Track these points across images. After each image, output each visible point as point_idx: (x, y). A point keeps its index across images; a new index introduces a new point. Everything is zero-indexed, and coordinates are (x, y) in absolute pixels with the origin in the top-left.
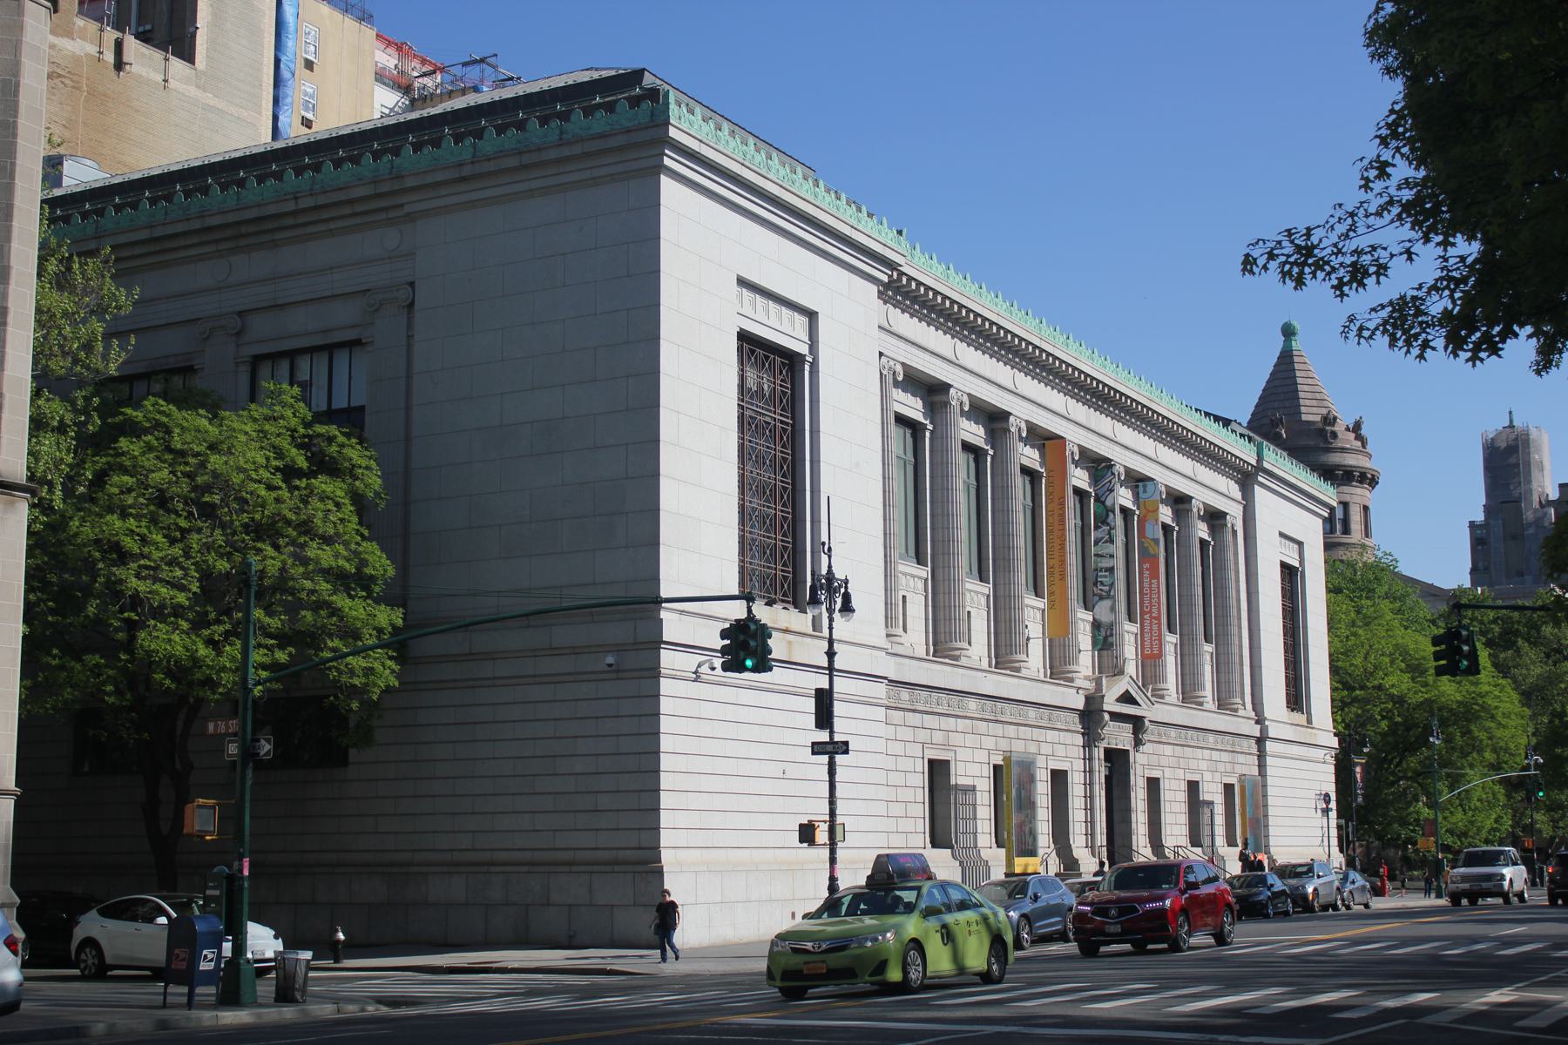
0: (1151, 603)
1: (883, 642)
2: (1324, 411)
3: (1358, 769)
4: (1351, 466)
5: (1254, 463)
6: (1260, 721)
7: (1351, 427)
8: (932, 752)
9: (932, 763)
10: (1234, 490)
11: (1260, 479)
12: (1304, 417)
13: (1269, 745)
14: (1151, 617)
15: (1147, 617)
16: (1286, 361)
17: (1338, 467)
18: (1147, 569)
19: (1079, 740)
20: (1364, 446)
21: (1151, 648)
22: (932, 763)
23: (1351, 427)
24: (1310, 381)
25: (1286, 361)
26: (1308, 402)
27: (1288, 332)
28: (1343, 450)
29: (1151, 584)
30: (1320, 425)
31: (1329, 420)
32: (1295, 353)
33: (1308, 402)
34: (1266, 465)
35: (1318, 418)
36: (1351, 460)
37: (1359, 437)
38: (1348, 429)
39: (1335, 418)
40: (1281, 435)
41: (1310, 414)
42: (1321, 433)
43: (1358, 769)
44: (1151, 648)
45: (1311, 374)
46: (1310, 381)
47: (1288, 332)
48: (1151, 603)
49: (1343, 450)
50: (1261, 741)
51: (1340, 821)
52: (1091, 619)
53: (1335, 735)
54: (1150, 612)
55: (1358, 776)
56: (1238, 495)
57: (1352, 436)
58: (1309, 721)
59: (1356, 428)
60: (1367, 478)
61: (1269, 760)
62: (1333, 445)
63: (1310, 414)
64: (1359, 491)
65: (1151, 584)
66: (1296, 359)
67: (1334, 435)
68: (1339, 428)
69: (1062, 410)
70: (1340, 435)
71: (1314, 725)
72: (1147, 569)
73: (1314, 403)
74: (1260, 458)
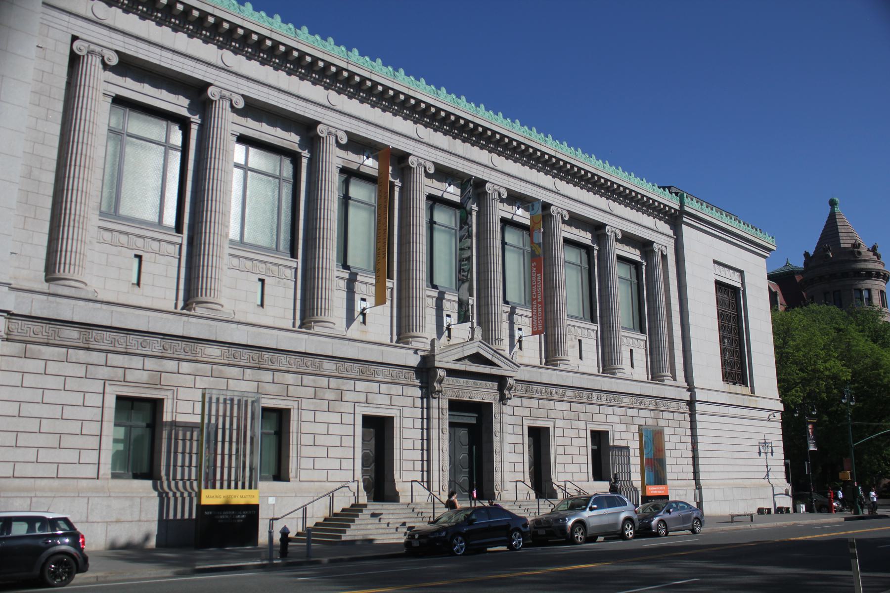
0: (537, 292)
1: (45, 287)
2: (853, 242)
3: (810, 426)
4: (870, 269)
5: (677, 207)
6: (691, 389)
7: (870, 249)
8: (528, 422)
9: (369, 421)
10: (666, 228)
11: (685, 219)
12: (842, 246)
13: (698, 407)
14: (537, 302)
15: (534, 303)
16: (832, 219)
17: (862, 270)
18: (535, 267)
19: (418, 392)
20: (878, 259)
21: (537, 326)
22: (369, 421)
23: (870, 249)
24: (846, 227)
25: (832, 218)
26: (844, 238)
27: (833, 203)
28: (865, 261)
29: (537, 277)
30: (852, 249)
31: (856, 246)
32: (836, 214)
33: (844, 238)
34: (686, 209)
35: (850, 246)
36: (870, 266)
37: (875, 254)
38: (869, 250)
39: (859, 244)
40: (829, 256)
41: (845, 243)
42: (852, 253)
43: (810, 426)
44: (537, 326)
45: (846, 224)
46: (846, 227)
47: (833, 203)
48: (537, 292)
49: (865, 261)
50: (691, 403)
51: (787, 461)
52: (456, 299)
53: (781, 402)
54: (537, 299)
55: (810, 431)
56: (671, 233)
57: (871, 254)
58: (753, 391)
59: (874, 249)
60: (881, 275)
61: (698, 417)
62: (860, 259)
63: (845, 243)
64: (877, 282)
65: (537, 277)
66: (837, 217)
67: (859, 253)
68: (863, 249)
69: (652, 226)
70: (863, 253)
71: (756, 394)
72: (535, 267)
73: (848, 238)
74: (682, 204)
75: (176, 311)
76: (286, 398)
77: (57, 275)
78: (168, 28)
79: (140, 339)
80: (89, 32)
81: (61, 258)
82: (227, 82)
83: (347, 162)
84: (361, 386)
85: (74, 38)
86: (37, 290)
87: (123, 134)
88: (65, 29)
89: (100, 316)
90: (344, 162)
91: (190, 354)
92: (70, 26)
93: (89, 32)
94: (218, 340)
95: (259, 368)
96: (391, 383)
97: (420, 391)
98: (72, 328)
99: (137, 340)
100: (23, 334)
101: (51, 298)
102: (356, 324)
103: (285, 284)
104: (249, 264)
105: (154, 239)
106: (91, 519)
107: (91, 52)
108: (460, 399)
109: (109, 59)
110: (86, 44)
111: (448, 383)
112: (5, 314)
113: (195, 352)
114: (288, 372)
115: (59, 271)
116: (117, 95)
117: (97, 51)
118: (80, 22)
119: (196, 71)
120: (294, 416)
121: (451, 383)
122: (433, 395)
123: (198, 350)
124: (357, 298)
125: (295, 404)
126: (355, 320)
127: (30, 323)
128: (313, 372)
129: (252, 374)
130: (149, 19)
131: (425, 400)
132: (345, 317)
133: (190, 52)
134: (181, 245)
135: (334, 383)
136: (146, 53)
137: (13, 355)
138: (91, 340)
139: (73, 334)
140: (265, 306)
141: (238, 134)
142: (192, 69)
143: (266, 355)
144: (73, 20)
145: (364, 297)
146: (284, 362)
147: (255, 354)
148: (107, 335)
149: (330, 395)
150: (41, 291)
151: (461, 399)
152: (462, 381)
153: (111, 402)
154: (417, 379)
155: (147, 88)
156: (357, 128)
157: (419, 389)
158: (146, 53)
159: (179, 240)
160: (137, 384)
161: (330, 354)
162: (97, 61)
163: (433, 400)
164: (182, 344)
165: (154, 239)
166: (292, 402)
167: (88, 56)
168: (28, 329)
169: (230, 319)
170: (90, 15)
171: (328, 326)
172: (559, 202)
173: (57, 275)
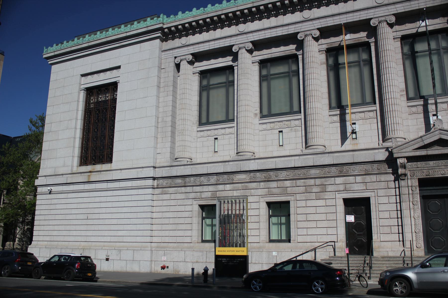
19: (392, 177)
75: (380, 147)
76: (367, 191)
77: (387, 137)
78: (342, 3)
79: (206, 178)
80: (180, 52)
81: (388, 128)
82: (242, 39)
83: (330, 44)
84: (339, 180)
85: (175, 57)
86: (165, 166)
87: (440, 49)
88: (172, 56)
89: (270, 164)
90: (328, 45)
91: (230, 180)
92: (173, 54)
93: (180, 52)
94: (242, 170)
95: (268, 181)
96: (365, 175)
97: (394, 176)
98: (179, 179)
99: (337, 169)
100: (335, 173)
101: (171, 168)
102: (348, 142)
103: (295, 130)
104: (272, 125)
105: (222, 128)
106: (186, 260)
107: (306, 36)
108: (430, 177)
109: (315, 35)
110: (377, 19)
111: (416, 167)
112: (152, 178)
113: (232, 179)
114: (286, 180)
115: (388, 135)
116: (260, 60)
117: (383, 20)
118: (177, 50)
119: (335, 21)
120: (372, 201)
121: (419, 166)
122: (401, 177)
123: (234, 177)
124: (348, 124)
125: (373, 194)
126: (347, 138)
127: (164, 180)
128: (304, 177)
129: (264, 185)
130: (232, 26)
131: (397, 182)
132: (340, 138)
133: (279, 24)
134: (376, 110)
135: (318, 181)
136: (203, 47)
137: (159, 193)
138: (186, 182)
139: (179, 181)
140: (357, 138)
141: (401, 36)
142: (270, 34)
143: (271, 173)
144: (174, 51)
145: (216, 137)
146: (282, 175)
147: (338, 168)
148: (192, 179)
149: (315, 189)
150: (167, 166)
151: (432, 176)
152: (431, 163)
153: (341, 203)
154: (389, 168)
155: (213, 61)
156: (326, 23)
157: (391, 175)
158: (203, 47)
159: (374, 108)
160: (206, 199)
161: (312, 164)
162: (310, 38)
163: (402, 181)
164: (225, 176)
165: (222, 128)
166: (290, 197)
167: (379, 24)
168: (349, 169)
169: (249, 158)
170: (238, 33)
171: (314, 148)
172: (382, 12)
173: (387, 137)
